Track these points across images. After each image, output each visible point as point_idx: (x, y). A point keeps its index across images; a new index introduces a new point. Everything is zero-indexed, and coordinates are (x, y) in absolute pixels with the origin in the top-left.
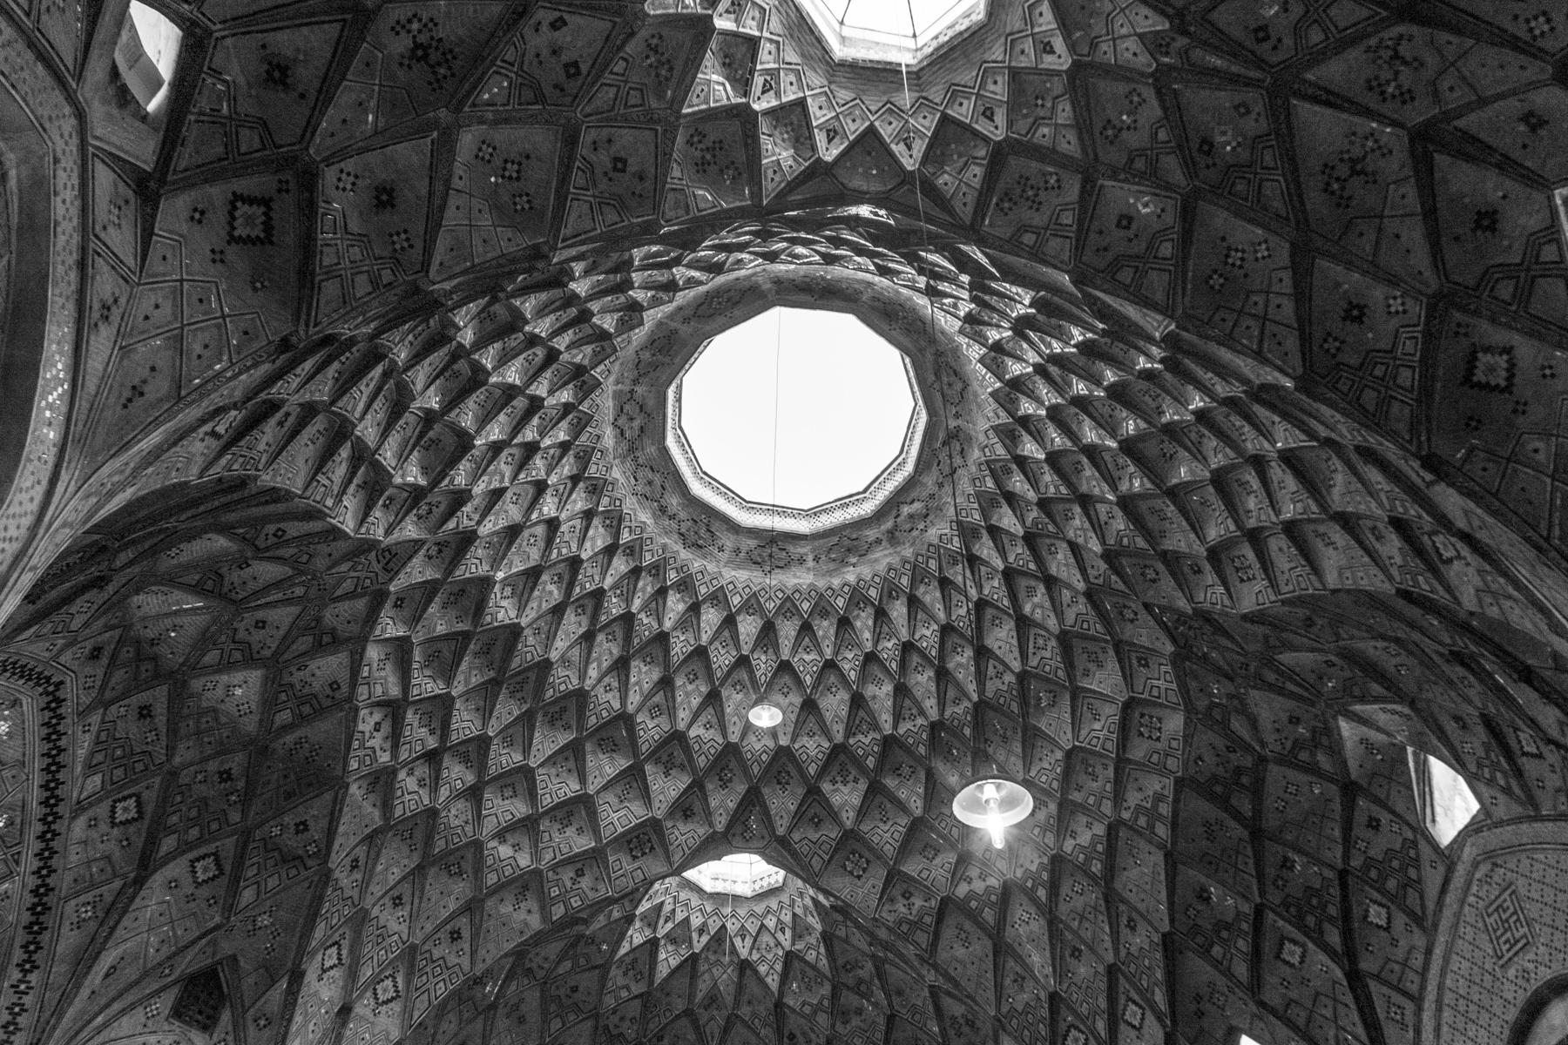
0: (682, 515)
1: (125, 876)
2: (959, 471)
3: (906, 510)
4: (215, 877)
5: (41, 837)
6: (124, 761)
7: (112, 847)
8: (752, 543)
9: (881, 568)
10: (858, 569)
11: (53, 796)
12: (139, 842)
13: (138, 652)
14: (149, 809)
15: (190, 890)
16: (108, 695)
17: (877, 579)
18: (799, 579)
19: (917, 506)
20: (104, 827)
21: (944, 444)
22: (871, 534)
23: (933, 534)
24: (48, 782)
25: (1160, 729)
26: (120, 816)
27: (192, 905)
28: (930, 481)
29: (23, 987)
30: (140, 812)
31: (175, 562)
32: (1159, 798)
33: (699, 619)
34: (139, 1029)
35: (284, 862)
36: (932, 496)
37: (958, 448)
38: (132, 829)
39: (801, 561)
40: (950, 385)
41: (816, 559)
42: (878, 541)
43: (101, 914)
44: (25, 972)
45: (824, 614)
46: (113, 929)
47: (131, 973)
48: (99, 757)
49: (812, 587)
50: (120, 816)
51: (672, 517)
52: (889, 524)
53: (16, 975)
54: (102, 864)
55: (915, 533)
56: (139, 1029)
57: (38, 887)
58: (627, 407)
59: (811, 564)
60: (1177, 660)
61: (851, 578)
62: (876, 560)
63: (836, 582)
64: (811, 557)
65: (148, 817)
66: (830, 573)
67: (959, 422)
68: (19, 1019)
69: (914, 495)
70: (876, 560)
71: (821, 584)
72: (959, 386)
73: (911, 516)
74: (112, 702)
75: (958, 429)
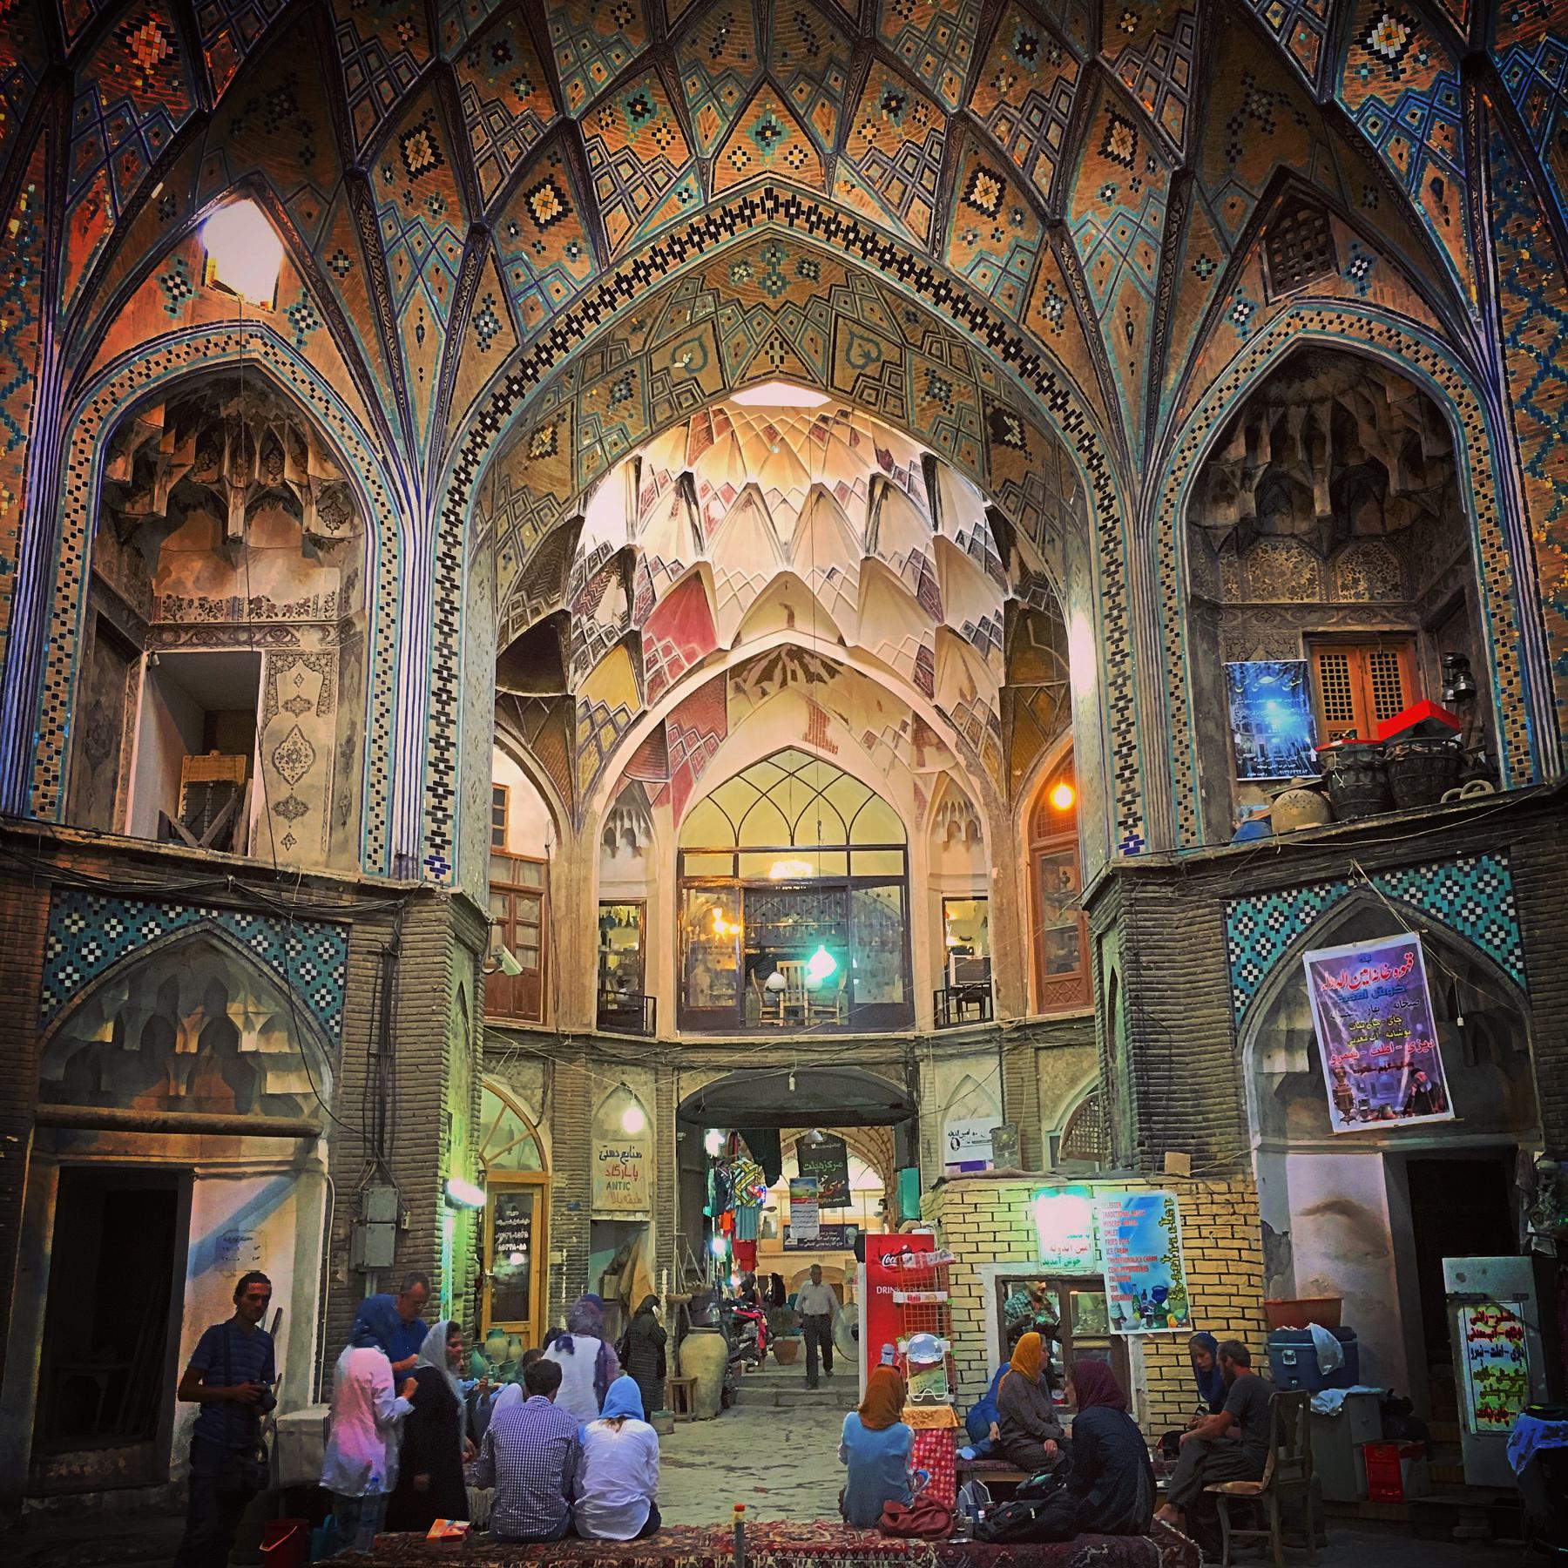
1: (1043, 245)
4: (1134, 137)
5: (939, 300)
6: (922, 163)
7: (1013, 234)
11: (901, 264)
12: (1023, 204)
13: (809, 78)
14: (998, 170)
15: (1129, 173)
16: (828, 145)
20: (987, 228)
24: (881, 258)
26: (989, 203)
27: (1142, 188)
29: (1073, 421)
30: (998, 179)
31: (640, 18)
34: (1241, 341)
35: (1172, 37)
38: (1008, 198)
43: (1066, 297)
44: (1062, 407)
46: (1087, 297)
47: (1146, 312)
48: (894, 193)
50: (989, 203)
53: (1059, 416)
54: (1018, 258)
56: (1241, 341)
57: (990, 335)
65: (1004, 175)
68: (1095, 449)
74: (840, 145)
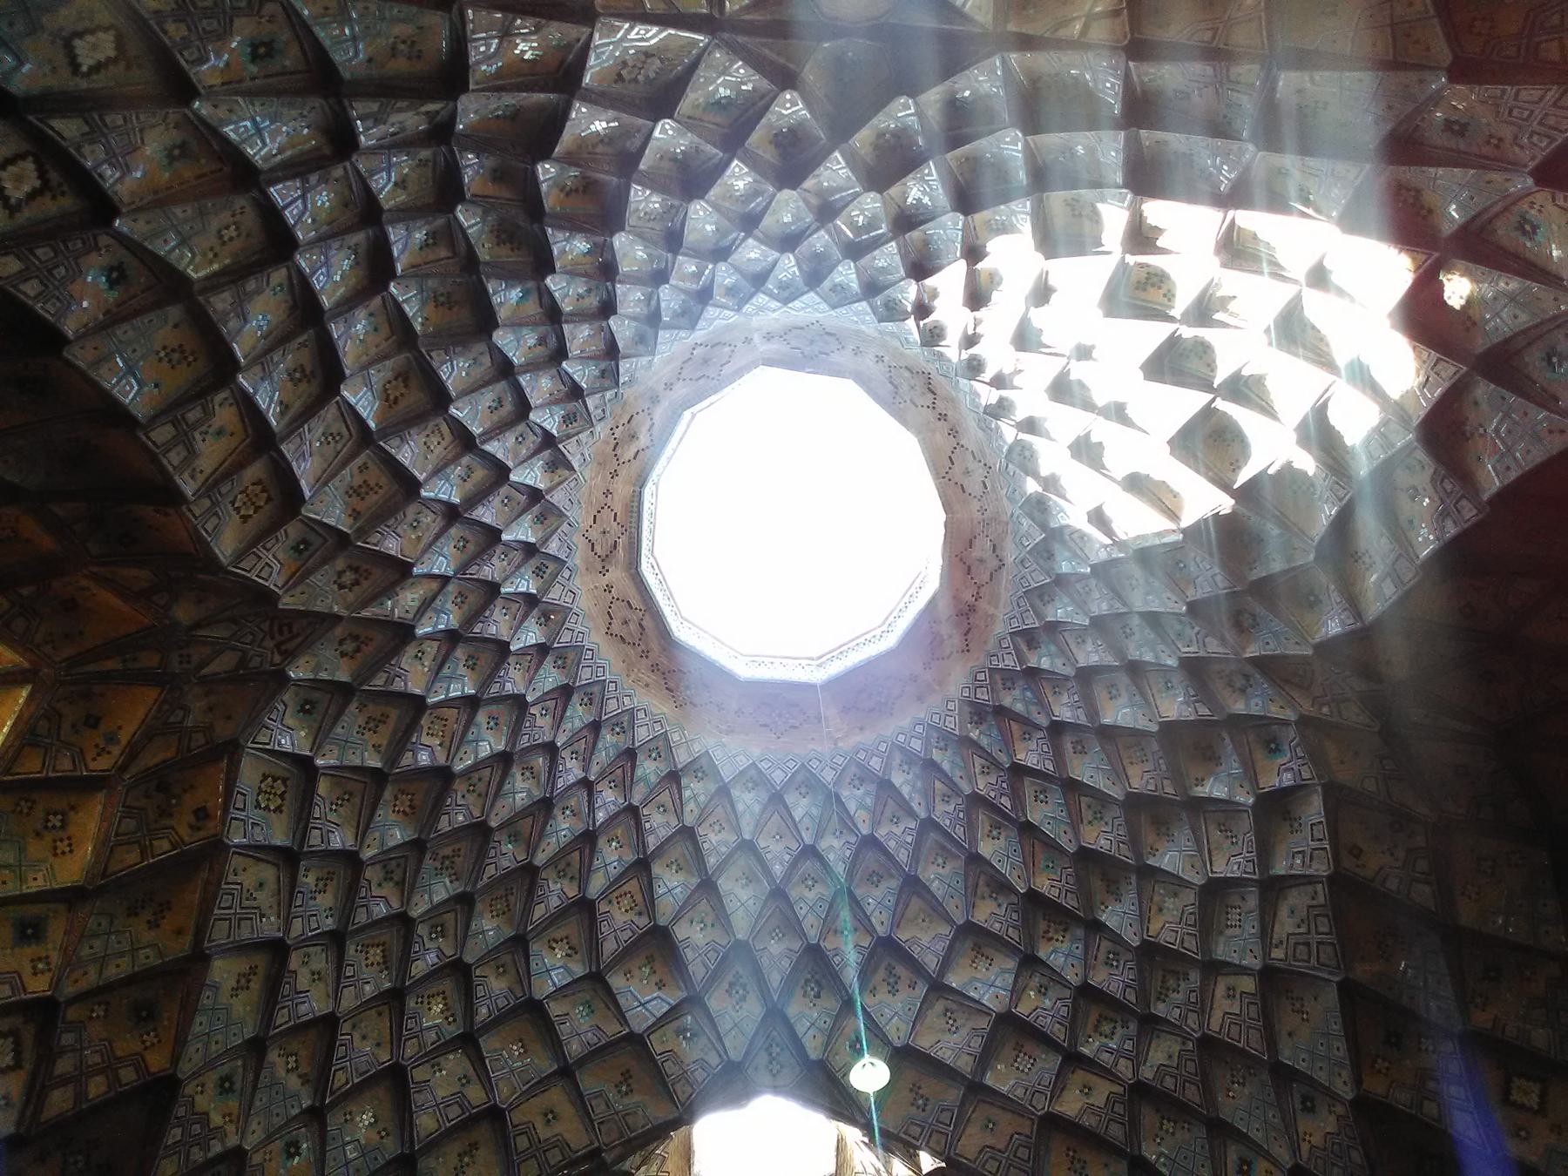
18: (766, 313)
25: (238, 510)
32: (192, 453)
36: (615, 474)
37: (598, 548)
39: (769, 337)
41: (748, 340)
42: (669, 386)
58: (986, 577)
60: (265, 597)
67: (605, 581)
72: (616, 628)
75: (604, 571)
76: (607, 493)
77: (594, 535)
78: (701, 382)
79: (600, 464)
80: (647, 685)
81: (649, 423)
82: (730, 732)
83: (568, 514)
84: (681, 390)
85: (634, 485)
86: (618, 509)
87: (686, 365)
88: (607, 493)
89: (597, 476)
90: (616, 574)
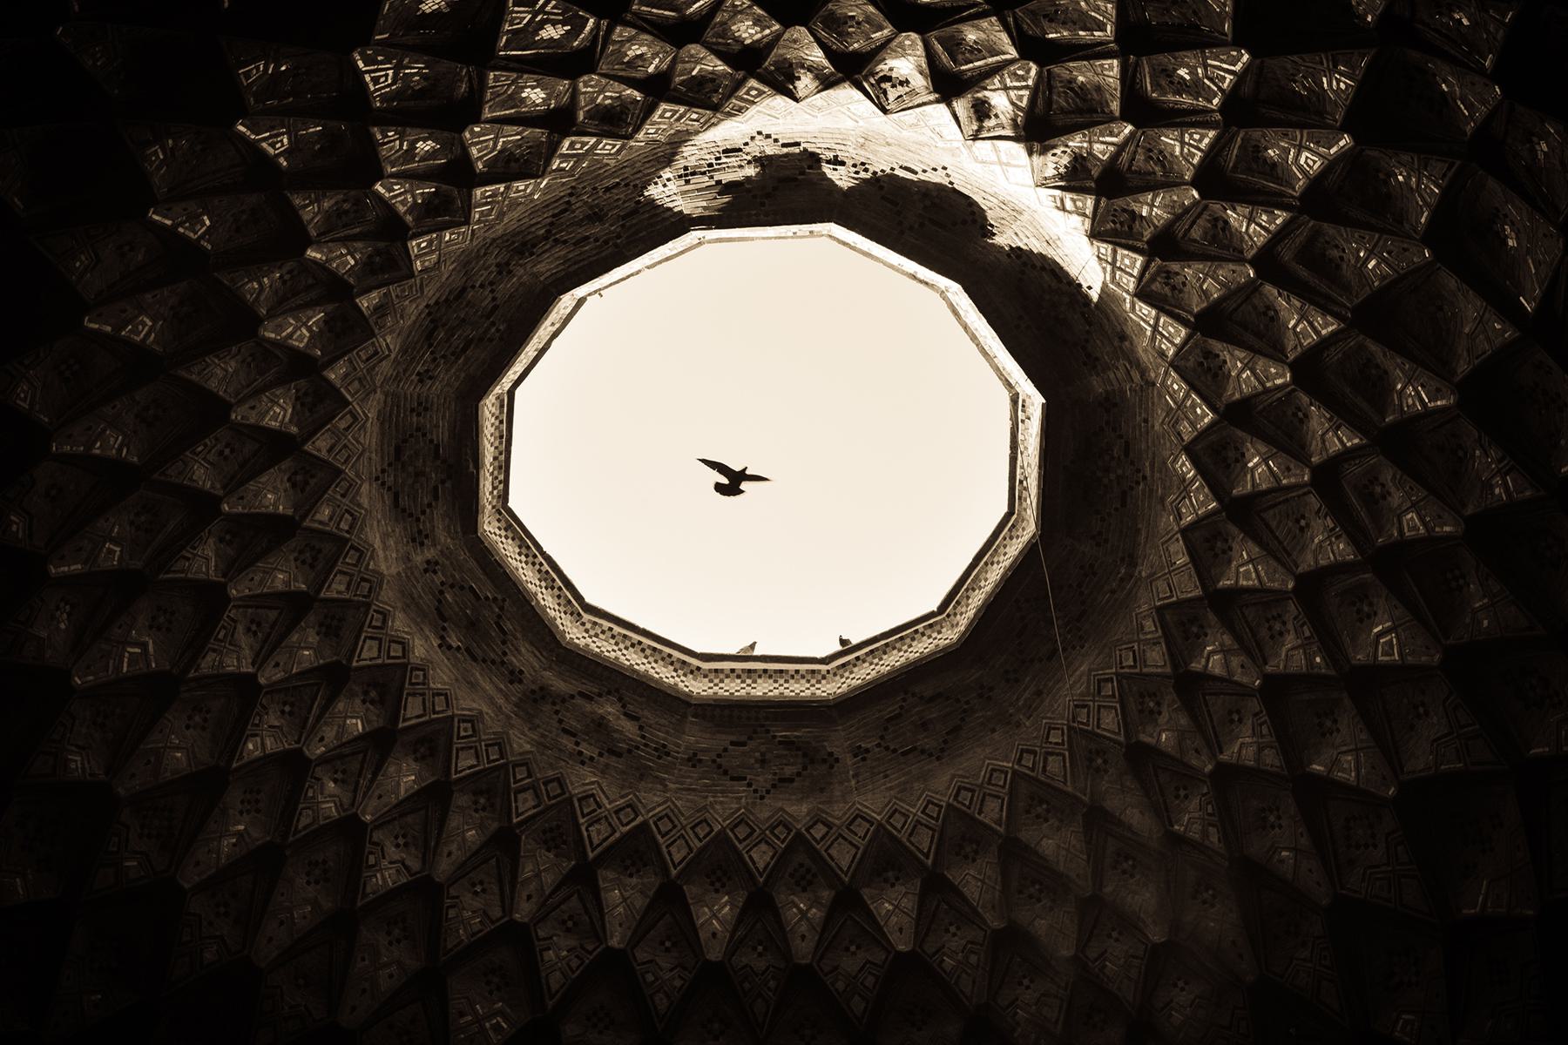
0: (507, 287)
2: (740, 787)
3: (608, 709)
8: (442, 434)
9: (467, 703)
10: (439, 656)
17: (440, 703)
19: (629, 728)
21: (788, 743)
22: (525, 658)
23: (583, 780)
28: (693, 737)
33: (280, 381)
36: (662, 751)
37: (789, 771)
39: (419, 538)
40: (924, 725)
41: (431, 566)
42: (515, 676)
45: (330, 630)
49: (375, 582)
51: (504, 269)
52: (559, 685)
55: (567, 742)
59: (419, 559)
61: (421, 648)
62: (473, 685)
63: (400, 623)
64: (430, 554)
66: (411, 603)
67: (849, 760)
69: (648, 715)
70: (473, 685)
71: (388, 596)
73: (600, 724)
75: (831, 760)
76: (693, 760)
77: (763, 779)
78: (508, 626)
79: (642, 777)
80: (1039, 693)
81: (579, 701)
82: (1132, 561)
83: (717, 828)
84: (525, 658)
85: (684, 716)
86: (724, 740)
87: (479, 653)
88: (693, 760)
89: (662, 782)
90: (837, 742)
